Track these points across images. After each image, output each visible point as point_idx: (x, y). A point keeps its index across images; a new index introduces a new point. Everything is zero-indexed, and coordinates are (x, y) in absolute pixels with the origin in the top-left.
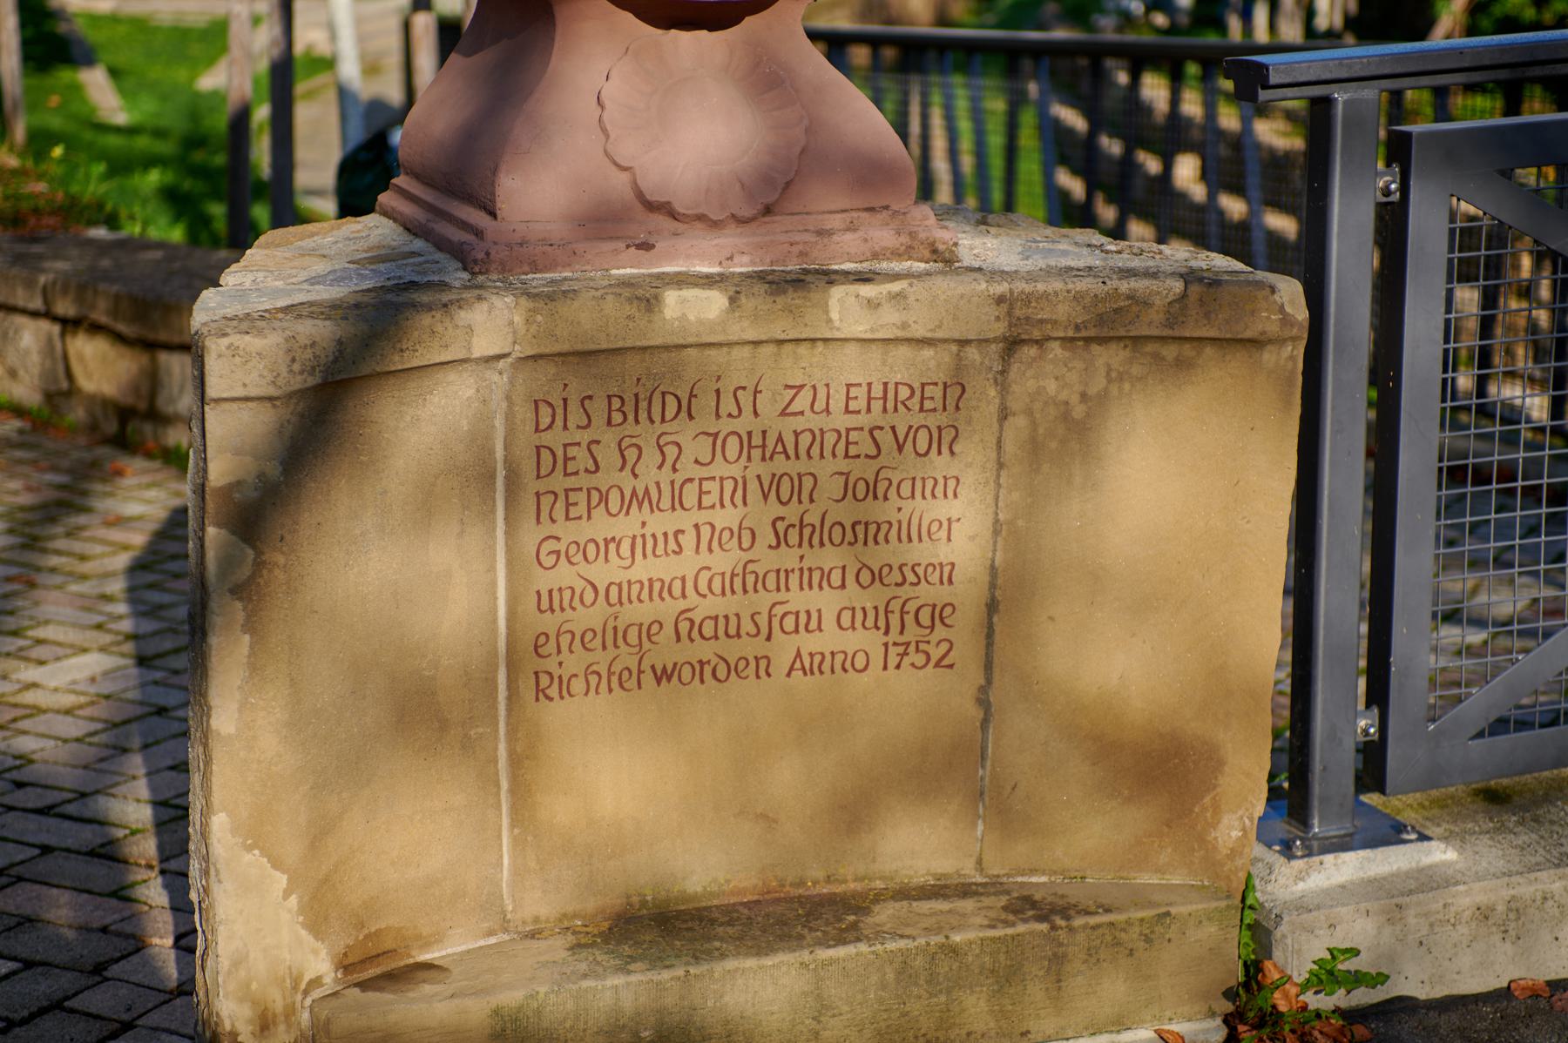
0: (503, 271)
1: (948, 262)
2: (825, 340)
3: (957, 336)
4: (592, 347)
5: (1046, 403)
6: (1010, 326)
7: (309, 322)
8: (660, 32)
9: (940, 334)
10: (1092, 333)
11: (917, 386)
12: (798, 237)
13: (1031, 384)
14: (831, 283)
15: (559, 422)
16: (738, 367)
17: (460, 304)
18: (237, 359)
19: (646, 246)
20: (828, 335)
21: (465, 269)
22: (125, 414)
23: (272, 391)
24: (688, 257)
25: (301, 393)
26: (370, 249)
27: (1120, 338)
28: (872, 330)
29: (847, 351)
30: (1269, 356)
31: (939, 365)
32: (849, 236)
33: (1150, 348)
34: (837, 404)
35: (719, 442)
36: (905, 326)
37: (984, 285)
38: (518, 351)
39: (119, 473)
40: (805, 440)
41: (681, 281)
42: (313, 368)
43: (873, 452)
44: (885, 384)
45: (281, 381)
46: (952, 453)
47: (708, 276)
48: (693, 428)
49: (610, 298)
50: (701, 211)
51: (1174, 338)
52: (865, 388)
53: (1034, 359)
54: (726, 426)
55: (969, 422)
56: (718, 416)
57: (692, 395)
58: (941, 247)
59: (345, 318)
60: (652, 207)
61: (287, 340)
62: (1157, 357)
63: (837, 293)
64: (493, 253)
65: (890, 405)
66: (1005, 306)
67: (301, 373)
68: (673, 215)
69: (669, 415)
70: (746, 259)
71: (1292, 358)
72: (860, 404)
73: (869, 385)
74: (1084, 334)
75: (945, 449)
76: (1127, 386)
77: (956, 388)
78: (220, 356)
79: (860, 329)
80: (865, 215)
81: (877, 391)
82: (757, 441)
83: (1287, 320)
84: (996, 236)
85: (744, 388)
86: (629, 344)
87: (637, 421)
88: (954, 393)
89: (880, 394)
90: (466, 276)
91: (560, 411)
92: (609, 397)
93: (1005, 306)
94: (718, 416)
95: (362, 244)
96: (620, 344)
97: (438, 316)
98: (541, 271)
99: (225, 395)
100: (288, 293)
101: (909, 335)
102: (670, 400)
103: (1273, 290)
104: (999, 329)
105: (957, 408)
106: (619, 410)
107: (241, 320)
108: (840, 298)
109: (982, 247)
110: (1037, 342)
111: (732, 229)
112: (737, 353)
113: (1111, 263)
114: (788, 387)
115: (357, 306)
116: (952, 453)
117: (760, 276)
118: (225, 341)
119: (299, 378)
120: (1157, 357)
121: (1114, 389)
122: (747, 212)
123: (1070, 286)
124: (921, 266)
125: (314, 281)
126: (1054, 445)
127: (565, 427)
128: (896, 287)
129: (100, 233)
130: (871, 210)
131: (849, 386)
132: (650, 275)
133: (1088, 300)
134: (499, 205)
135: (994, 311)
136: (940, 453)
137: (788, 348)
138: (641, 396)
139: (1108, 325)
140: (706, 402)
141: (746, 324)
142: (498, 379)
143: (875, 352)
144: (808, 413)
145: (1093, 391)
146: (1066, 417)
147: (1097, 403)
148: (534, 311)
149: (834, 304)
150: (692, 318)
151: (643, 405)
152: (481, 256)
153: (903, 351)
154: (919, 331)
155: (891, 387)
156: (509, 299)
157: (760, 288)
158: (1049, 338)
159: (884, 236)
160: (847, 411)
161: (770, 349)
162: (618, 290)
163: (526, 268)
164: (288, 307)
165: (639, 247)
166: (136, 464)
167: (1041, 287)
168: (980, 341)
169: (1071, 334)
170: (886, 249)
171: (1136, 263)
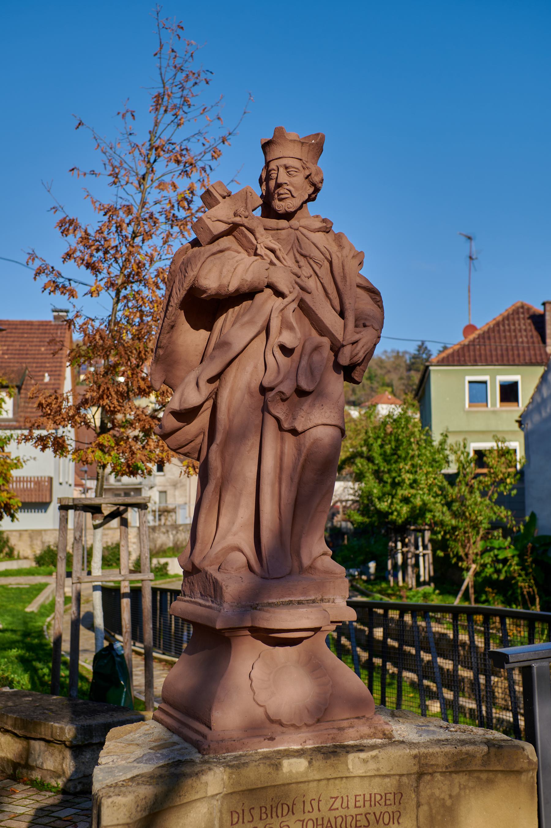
0: (215, 753)
1: (390, 738)
2: (347, 777)
3: (399, 773)
4: (255, 787)
5: (435, 800)
6: (420, 767)
7: (143, 787)
8: (271, 648)
9: (392, 773)
10: (453, 769)
11: (383, 794)
12: (331, 732)
13: (429, 791)
14: (348, 752)
15: (241, 820)
16: (312, 791)
17: (202, 772)
18: (115, 808)
19: (272, 739)
20: (348, 775)
21: (199, 752)
22: (15, 765)
23: (129, 821)
24: (288, 742)
25: (140, 820)
26: (155, 741)
27: (464, 771)
28: (365, 772)
29: (355, 781)
30: (523, 777)
31: (391, 785)
32: (351, 730)
33: (476, 775)
34: (352, 804)
35: (305, 824)
36: (378, 770)
37: (408, 751)
38: (225, 791)
39: (14, 792)
40: (339, 820)
41: (288, 754)
42: (145, 808)
43: (367, 824)
44: (371, 794)
45: (132, 816)
46: (399, 823)
47: (297, 751)
48: (294, 818)
49: (261, 765)
50: (293, 723)
51: (486, 771)
52: (362, 796)
53: (429, 781)
54: (307, 816)
55: (405, 809)
56: (304, 812)
57: (294, 804)
58: (387, 732)
59: (157, 784)
60: (272, 721)
61: (135, 798)
62: (478, 778)
63: (351, 756)
64: (211, 745)
65: (373, 803)
66: (417, 759)
67: (141, 811)
68: (281, 724)
69: (285, 813)
70: (311, 742)
72: (360, 804)
73: (364, 795)
74: (450, 770)
75: (396, 822)
76: (467, 791)
77: (399, 794)
78: (108, 807)
79: (360, 772)
80: (356, 720)
81: (367, 798)
82: (320, 822)
83: (530, 762)
84: (403, 723)
85: (314, 800)
86: (269, 784)
87: (272, 817)
88: (398, 797)
89: (369, 799)
90: (200, 756)
91: (241, 815)
92: (261, 808)
93: (417, 759)
94: (304, 812)
95: (152, 738)
96: (266, 785)
97: (194, 779)
98: (230, 752)
99: (109, 824)
100: (130, 769)
101: (380, 773)
102: (285, 807)
103: (524, 749)
104: (415, 769)
105: (400, 803)
106: (265, 813)
107: (115, 787)
108: (353, 759)
109: (402, 730)
110: (430, 774)
111: (304, 729)
112: (311, 784)
113: (455, 737)
114: (332, 798)
115: (161, 776)
116: (399, 823)
117: (318, 750)
118: (110, 800)
119: (140, 814)
120: (478, 778)
121: (462, 793)
122: (310, 722)
123: (443, 750)
124: (379, 741)
125: (138, 760)
126: (439, 818)
127: (243, 822)
128: (374, 753)
129: (7, 689)
130: (358, 718)
131: (356, 796)
132: (274, 752)
133: (450, 756)
134: (212, 724)
135: (413, 762)
136: (394, 823)
137: (331, 781)
138: (273, 806)
139: (459, 765)
140: (299, 807)
141: (315, 772)
142: (216, 803)
143: (366, 781)
144: (340, 808)
145: (454, 793)
146: (443, 805)
147: (456, 799)
148: (232, 773)
149: (350, 762)
150: (294, 771)
151: (274, 810)
152: (206, 747)
153: (377, 780)
154: (384, 772)
155: (373, 795)
156: (222, 769)
157: (320, 756)
158: (436, 772)
159: (365, 730)
160: (356, 807)
161: (324, 782)
162: (264, 761)
163: (224, 751)
164: (134, 777)
165: (269, 739)
166: (20, 787)
167: (431, 750)
168: (408, 774)
169: (444, 770)
170: (365, 734)
171: (464, 737)
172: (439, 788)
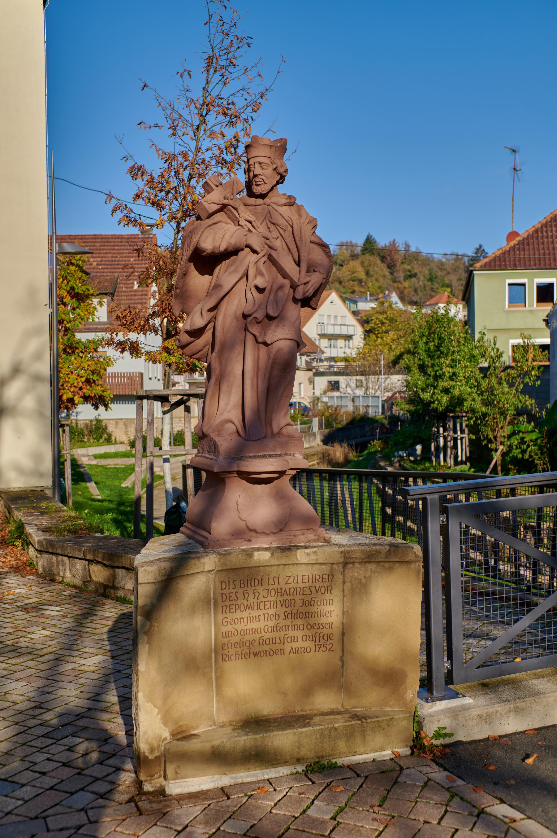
10: (366, 560)
16: (274, 572)
17: (202, 557)
19: (249, 541)
22: (105, 587)
23: (155, 581)
25: (162, 581)
30: (413, 566)
33: (381, 564)
34: (300, 580)
36: (317, 560)
38: (217, 569)
39: (104, 604)
40: (292, 590)
41: (259, 549)
48: (262, 588)
54: (271, 587)
60: (251, 530)
62: (383, 566)
63: (299, 552)
68: (256, 532)
69: (256, 584)
71: (419, 566)
72: (306, 581)
77: (331, 576)
79: (305, 561)
81: (311, 577)
82: (279, 591)
83: (417, 556)
88: (331, 577)
95: (176, 541)
100: (158, 555)
103: (413, 548)
104: (342, 560)
111: (272, 535)
117: (279, 548)
120: (383, 566)
121: (373, 575)
122: (275, 531)
125: (164, 552)
128: (314, 549)
130: (308, 529)
137: (287, 566)
139: (370, 557)
142: (211, 576)
143: (310, 567)
146: (360, 583)
147: (368, 579)
149: (298, 554)
153: (317, 566)
154: (321, 561)
156: (214, 555)
157: (279, 551)
159: (311, 536)
161: (282, 567)
167: (352, 549)
171: (377, 542)
172: (357, 572)
